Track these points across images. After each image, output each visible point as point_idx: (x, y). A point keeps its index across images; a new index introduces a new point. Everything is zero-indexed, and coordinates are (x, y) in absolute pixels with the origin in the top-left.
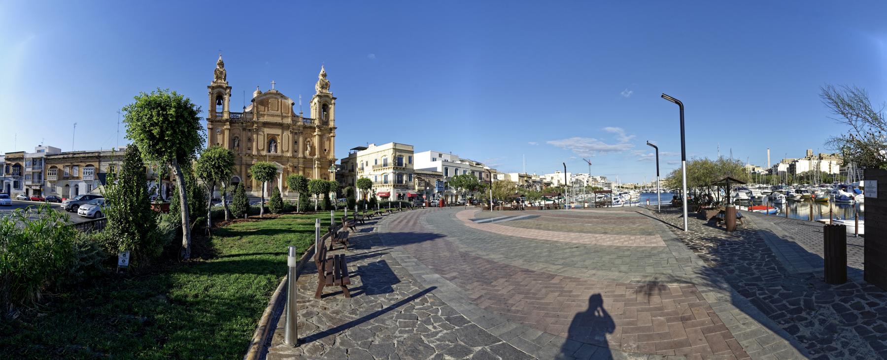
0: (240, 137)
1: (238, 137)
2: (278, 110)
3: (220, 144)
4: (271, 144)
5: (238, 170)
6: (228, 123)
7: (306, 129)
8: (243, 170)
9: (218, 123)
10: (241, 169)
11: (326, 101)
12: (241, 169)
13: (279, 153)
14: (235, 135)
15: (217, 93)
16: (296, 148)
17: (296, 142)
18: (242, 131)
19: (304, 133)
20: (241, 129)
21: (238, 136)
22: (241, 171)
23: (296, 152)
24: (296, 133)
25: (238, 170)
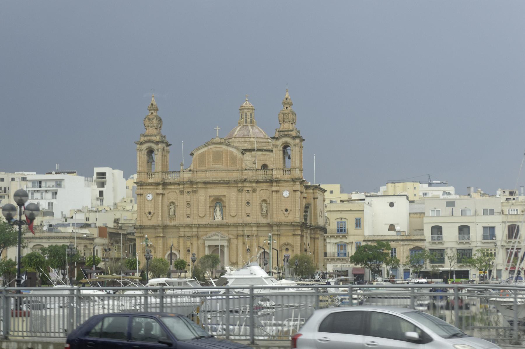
0: (176, 203)
1: (173, 203)
2: (222, 164)
3: (152, 213)
4: (215, 207)
5: (175, 244)
6: (161, 187)
7: (261, 185)
8: (181, 243)
9: (148, 187)
10: (178, 242)
11: (286, 143)
12: (178, 242)
13: (225, 221)
14: (171, 201)
15: (147, 149)
16: (248, 211)
17: (248, 203)
18: (179, 194)
19: (258, 189)
20: (178, 191)
21: (174, 201)
22: (179, 246)
23: (248, 216)
24: (248, 191)
25: (175, 244)
